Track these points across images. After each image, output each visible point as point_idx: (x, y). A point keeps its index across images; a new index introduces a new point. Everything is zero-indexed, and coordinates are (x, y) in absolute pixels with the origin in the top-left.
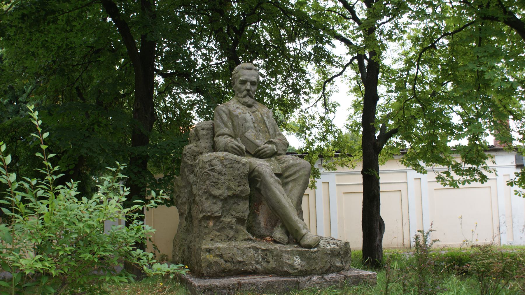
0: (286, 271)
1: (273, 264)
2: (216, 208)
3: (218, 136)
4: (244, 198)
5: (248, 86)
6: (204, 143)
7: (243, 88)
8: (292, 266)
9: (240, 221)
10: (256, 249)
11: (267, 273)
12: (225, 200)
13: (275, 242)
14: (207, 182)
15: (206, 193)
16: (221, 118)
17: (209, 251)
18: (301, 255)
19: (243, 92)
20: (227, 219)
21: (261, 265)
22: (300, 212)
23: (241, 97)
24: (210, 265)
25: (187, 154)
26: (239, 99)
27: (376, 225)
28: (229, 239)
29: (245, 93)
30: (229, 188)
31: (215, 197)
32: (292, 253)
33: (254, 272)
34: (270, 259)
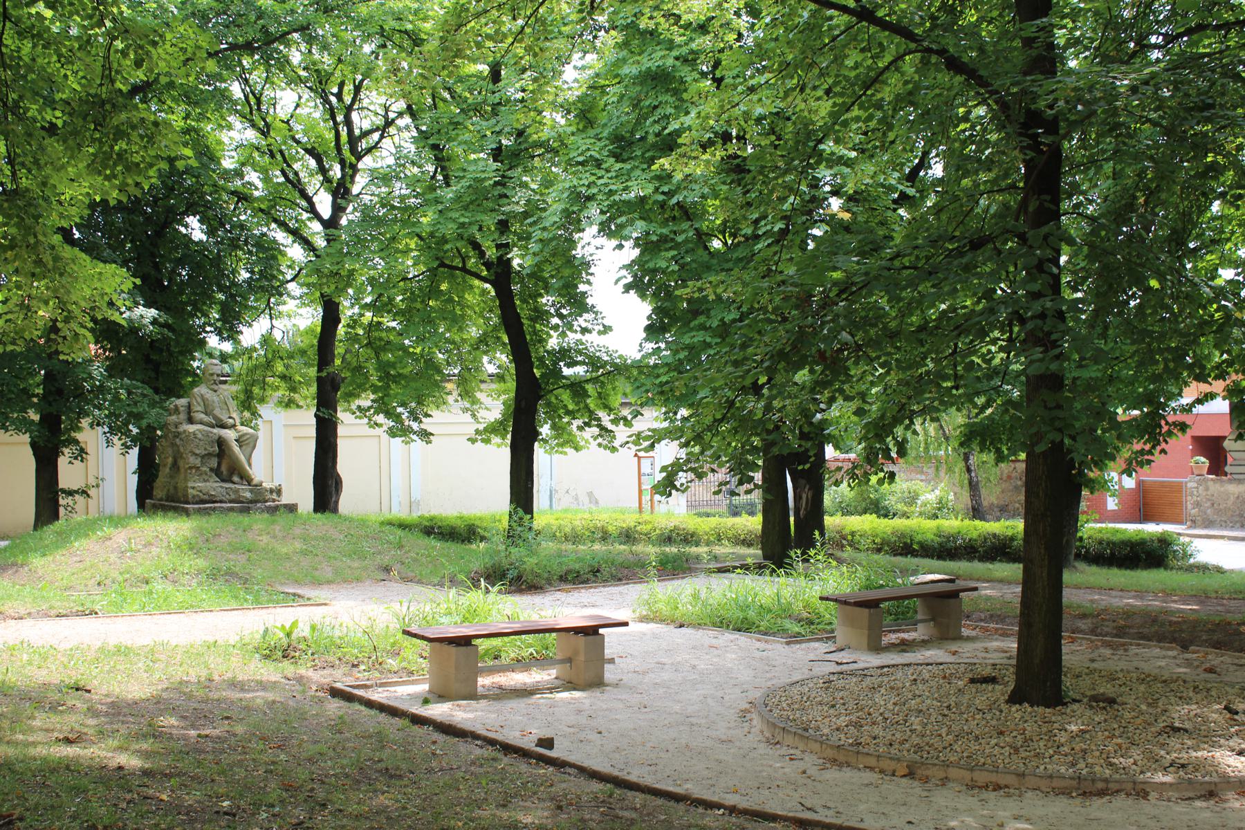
1: (233, 497)
2: (198, 462)
4: (215, 456)
5: (215, 377)
6: (183, 416)
9: (211, 470)
10: (221, 487)
11: (231, 502)
12: (203, 457)
13: (234, 483)
17: (193, 488)
18: (251, 491)
20: (204, 469)
22: (250, 465)
24: (194, 497)
27: (332, 483)
28: (205, 481)
30: (205, 449)
31: (196, 455)
32: (246, 490)
33: (221, 502)
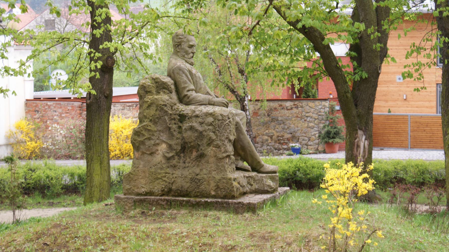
0: (267, 190)
1: (255, 186)
3: (188, 91)
7: (190, 50)
8: (269, 186)
14: (228, 131)
15: (227, 138)
16: (187, 76)
17: (235, 180)
19: (190, 54)
21: (248, 187)
23: (189, 58)
25: (168, 105)
26: (186, 59)
29: (191, 55)
34: (252, 183)
